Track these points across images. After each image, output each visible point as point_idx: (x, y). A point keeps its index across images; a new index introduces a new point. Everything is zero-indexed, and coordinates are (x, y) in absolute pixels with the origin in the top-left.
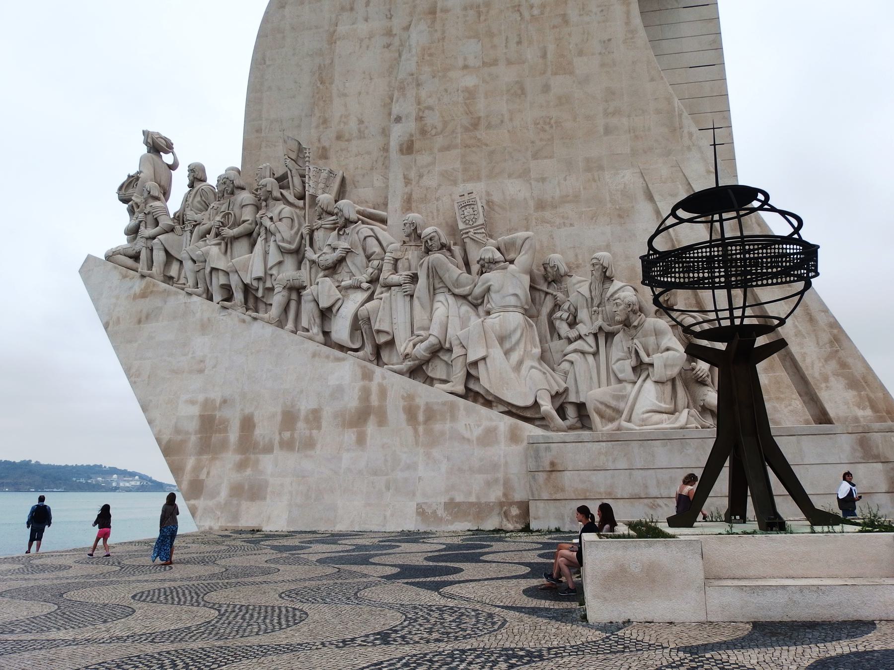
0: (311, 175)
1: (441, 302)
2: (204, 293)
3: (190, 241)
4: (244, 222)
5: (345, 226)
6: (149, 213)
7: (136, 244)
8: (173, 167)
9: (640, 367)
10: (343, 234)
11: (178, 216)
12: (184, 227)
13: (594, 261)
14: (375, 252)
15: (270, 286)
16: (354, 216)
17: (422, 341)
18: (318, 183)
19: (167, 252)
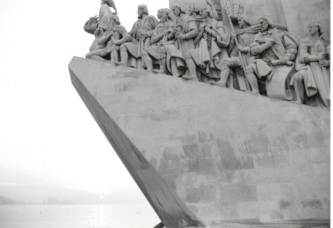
4: (191, 30)
5: (267, 30)
6: (116, 31)
7: (107, 49)
12: (138, 40)
14: (291, 44)
15: (214, 67)
18: (234, 11)
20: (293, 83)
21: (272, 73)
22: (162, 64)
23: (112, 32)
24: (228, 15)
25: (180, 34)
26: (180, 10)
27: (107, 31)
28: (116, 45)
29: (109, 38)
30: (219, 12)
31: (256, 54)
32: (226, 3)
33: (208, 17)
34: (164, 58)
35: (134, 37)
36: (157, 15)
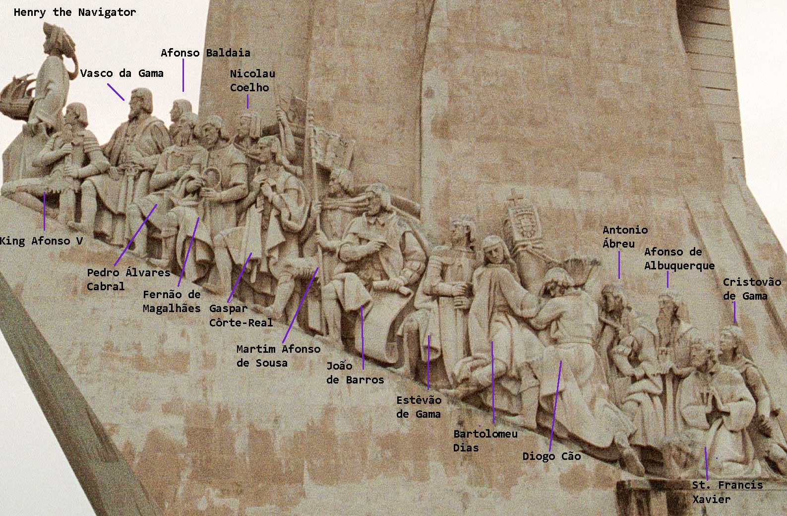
1: (503, 322)
3: (134, 190)
4: (235, 185)
5: (376, 215)
6: (78, 145)
7: (51, 182)
9: (716, 414)
10: (375, 223)
11: (110, 153)
12: (124, 170)
13: (666, 299)
14: (415, 251)
16: (389, 206)
17: (483, 366)
18: (326, 151)
19: (98, 198)
20: (403, 332)
21: (370, 306)
22: (166, 247)
24: (314, 162)
25: (211, 192)
26: (219, 133)
28: (74, 179)
29: (58, 158)
31: (349, 259)
32: (315, 131)
35: (114, 164)
36: (171, 113)
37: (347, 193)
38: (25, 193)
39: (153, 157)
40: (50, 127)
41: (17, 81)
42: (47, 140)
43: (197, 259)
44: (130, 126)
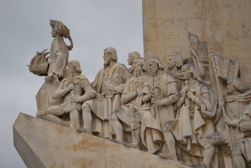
0: (216, 62)
2: (137, 146)
3: (112, 106)
4: (171, 94)
6: (77, 84)
7: (64, 107)
8: (70, 48)
12: (105, 95)
19: (93, 113)
22: (135, 135)
23: (71, 86)
24: (216, 75)
25: (157, 100)
26: (158, 65)
27: (65, 81)
28: (77, 103)
30: (206, 65)
31: (245, 130)
32: (214, 58)
33: (191, 78)
34: (137, 128)
35: (99, 92)
37: (238, 91)
38: (50, 115)
39: (121, 85)
40: (60, 76)
41: (39, 54)
42: (59, 84)
43: (154, 140)
44: (106, 70)
